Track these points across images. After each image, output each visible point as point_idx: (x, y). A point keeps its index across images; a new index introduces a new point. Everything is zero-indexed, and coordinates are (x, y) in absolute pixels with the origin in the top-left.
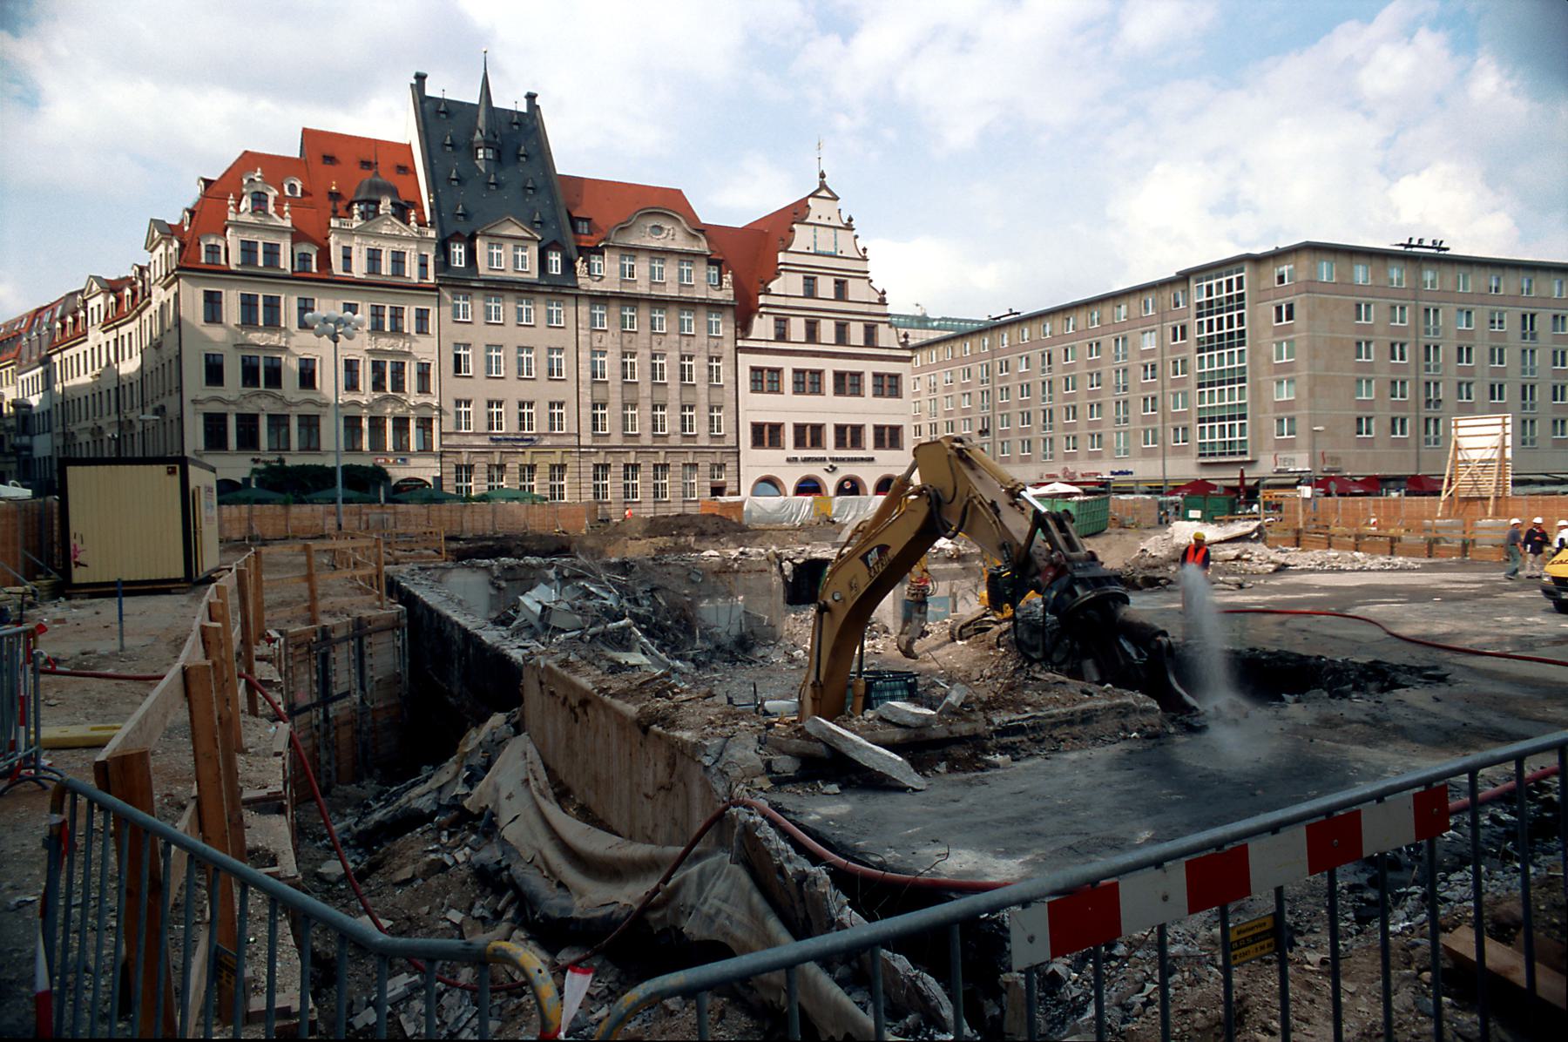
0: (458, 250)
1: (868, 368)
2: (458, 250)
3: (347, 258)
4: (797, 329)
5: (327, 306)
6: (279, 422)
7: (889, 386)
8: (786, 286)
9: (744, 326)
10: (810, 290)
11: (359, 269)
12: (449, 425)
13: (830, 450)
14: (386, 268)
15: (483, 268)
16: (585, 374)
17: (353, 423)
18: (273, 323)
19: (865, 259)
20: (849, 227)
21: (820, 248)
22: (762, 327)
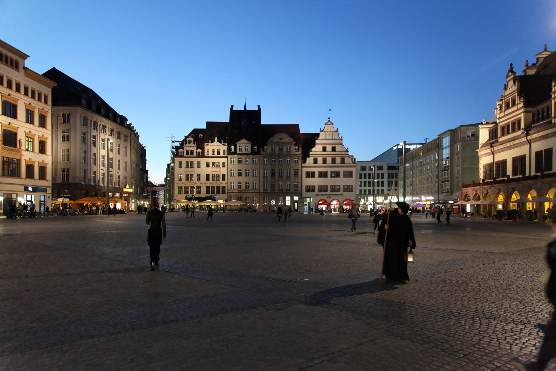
0: (232, 147)
1: (342, 170)
2: (232, 147)
3: (208, 151)
4: (320, 160)
5: (203, 161)
6: (192, 188)
7: (349, 174)
8: (317, 149)
9: (305, 161)
10: (324, 149)
11: (210, 154)
12: (229, 188)
13: (329, 192)
14: (216, 153)
15: (238, 152)
16: (262, 175)
17: (208, 188)
18: (192, 166)
19: (342, 139)
20: (337, 131)
21: (327, 138)
22: (310, 160)
